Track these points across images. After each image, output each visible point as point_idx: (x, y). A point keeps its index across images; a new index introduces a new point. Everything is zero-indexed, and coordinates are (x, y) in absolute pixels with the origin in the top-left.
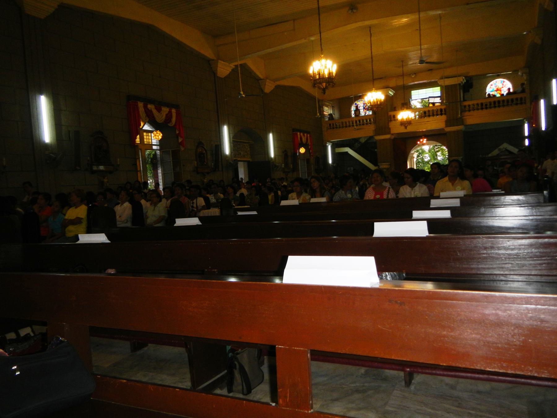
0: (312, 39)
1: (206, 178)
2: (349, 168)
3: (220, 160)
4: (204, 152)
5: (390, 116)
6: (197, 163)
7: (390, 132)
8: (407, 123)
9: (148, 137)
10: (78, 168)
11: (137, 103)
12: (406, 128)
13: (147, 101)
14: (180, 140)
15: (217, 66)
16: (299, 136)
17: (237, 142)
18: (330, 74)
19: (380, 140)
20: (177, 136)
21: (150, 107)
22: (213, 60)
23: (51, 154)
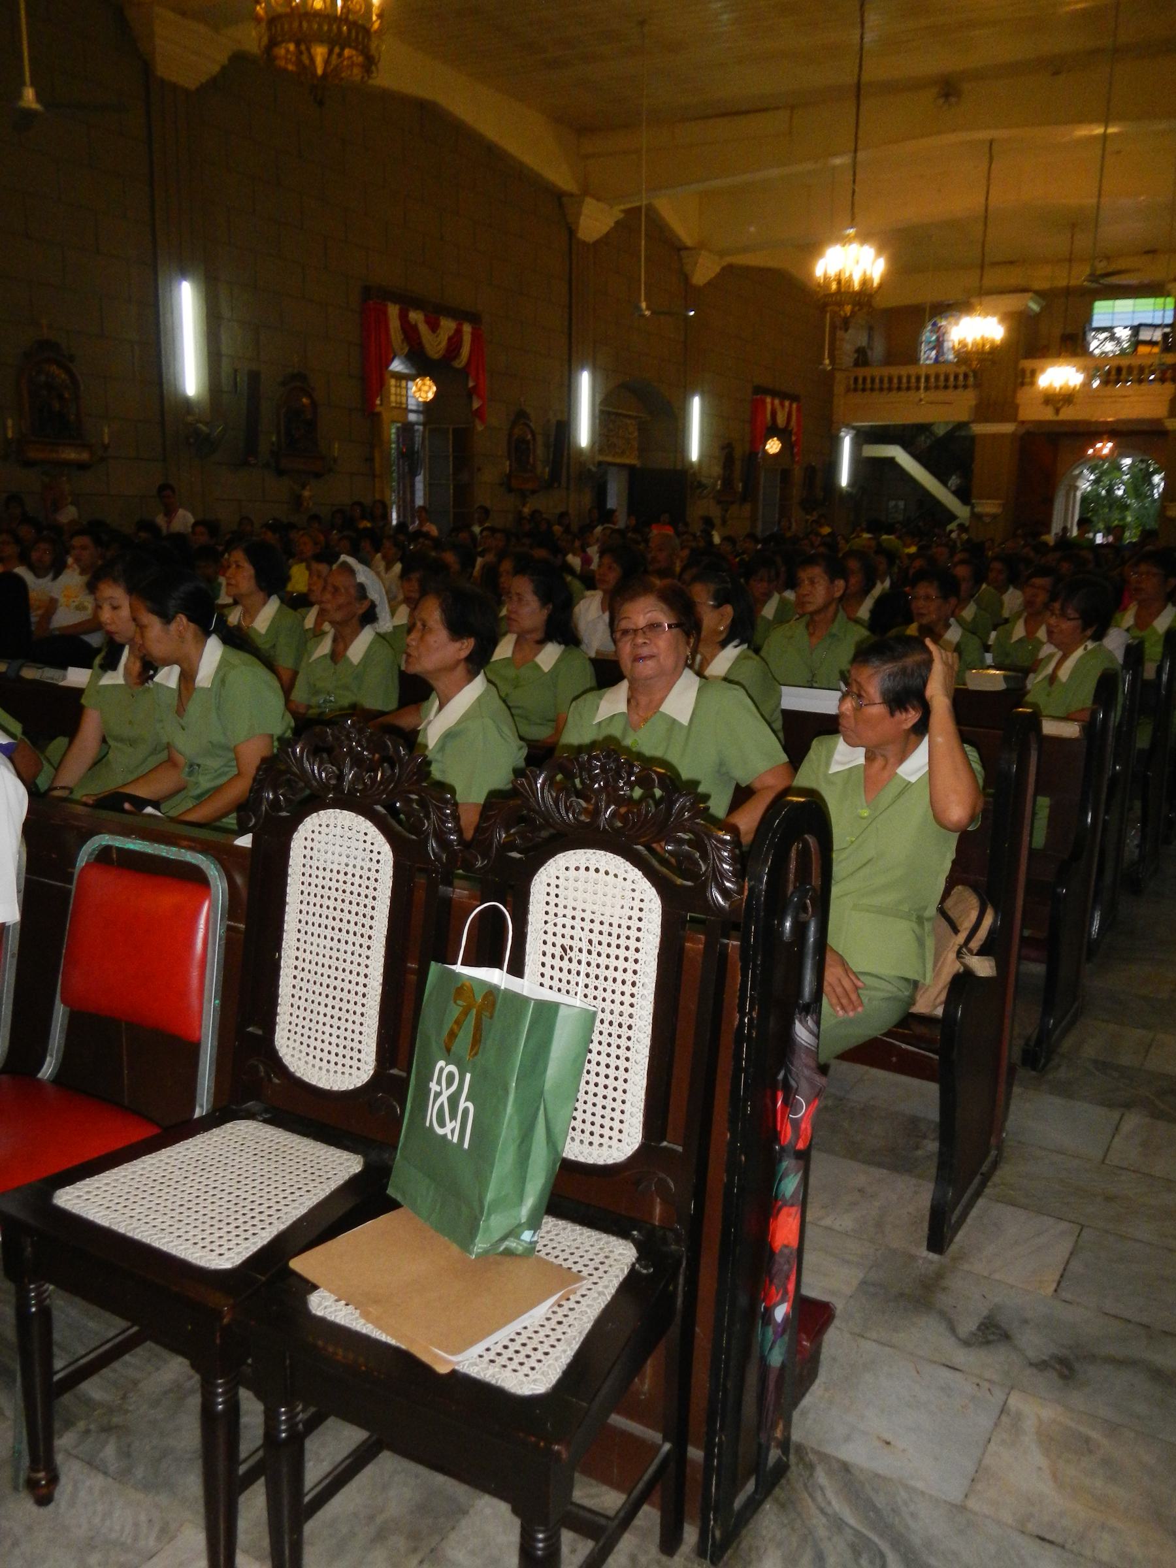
0: (838, 161)
1: (528, 505)
2: (892, 503)
3: (565, 459)
4: (529, 437)
5: (1023, 371)
6: (510, 466)
7: (1016, 415)
8: (1059, 399)
9: (399, 389)
10: (252, 460)
11: (386, 306)
12: (1057, 411)
13: (408, 302)
14: (476, 405)
15: (579, 214)
16: (769, 407)
17: (609, 413)
18: (865, 282)
19: (985, 436)
20: (470, 394)
21: (415, 316)
22: (571, 195)
23: (200, 425)
